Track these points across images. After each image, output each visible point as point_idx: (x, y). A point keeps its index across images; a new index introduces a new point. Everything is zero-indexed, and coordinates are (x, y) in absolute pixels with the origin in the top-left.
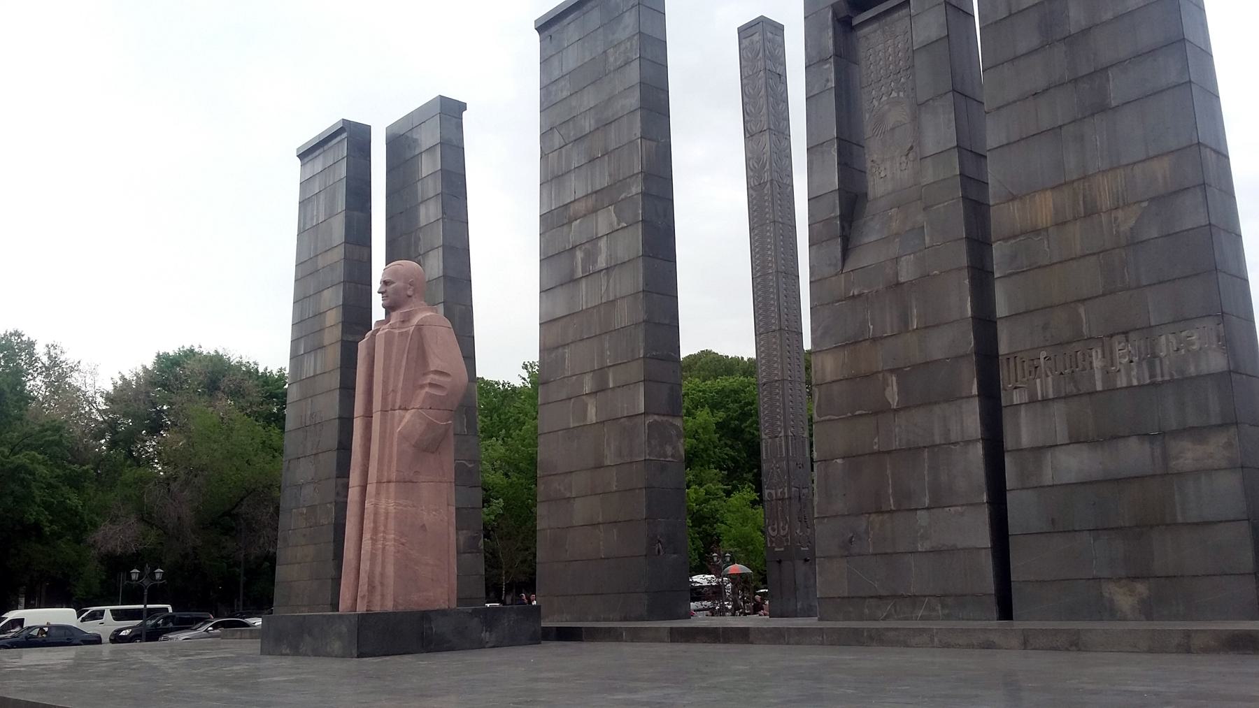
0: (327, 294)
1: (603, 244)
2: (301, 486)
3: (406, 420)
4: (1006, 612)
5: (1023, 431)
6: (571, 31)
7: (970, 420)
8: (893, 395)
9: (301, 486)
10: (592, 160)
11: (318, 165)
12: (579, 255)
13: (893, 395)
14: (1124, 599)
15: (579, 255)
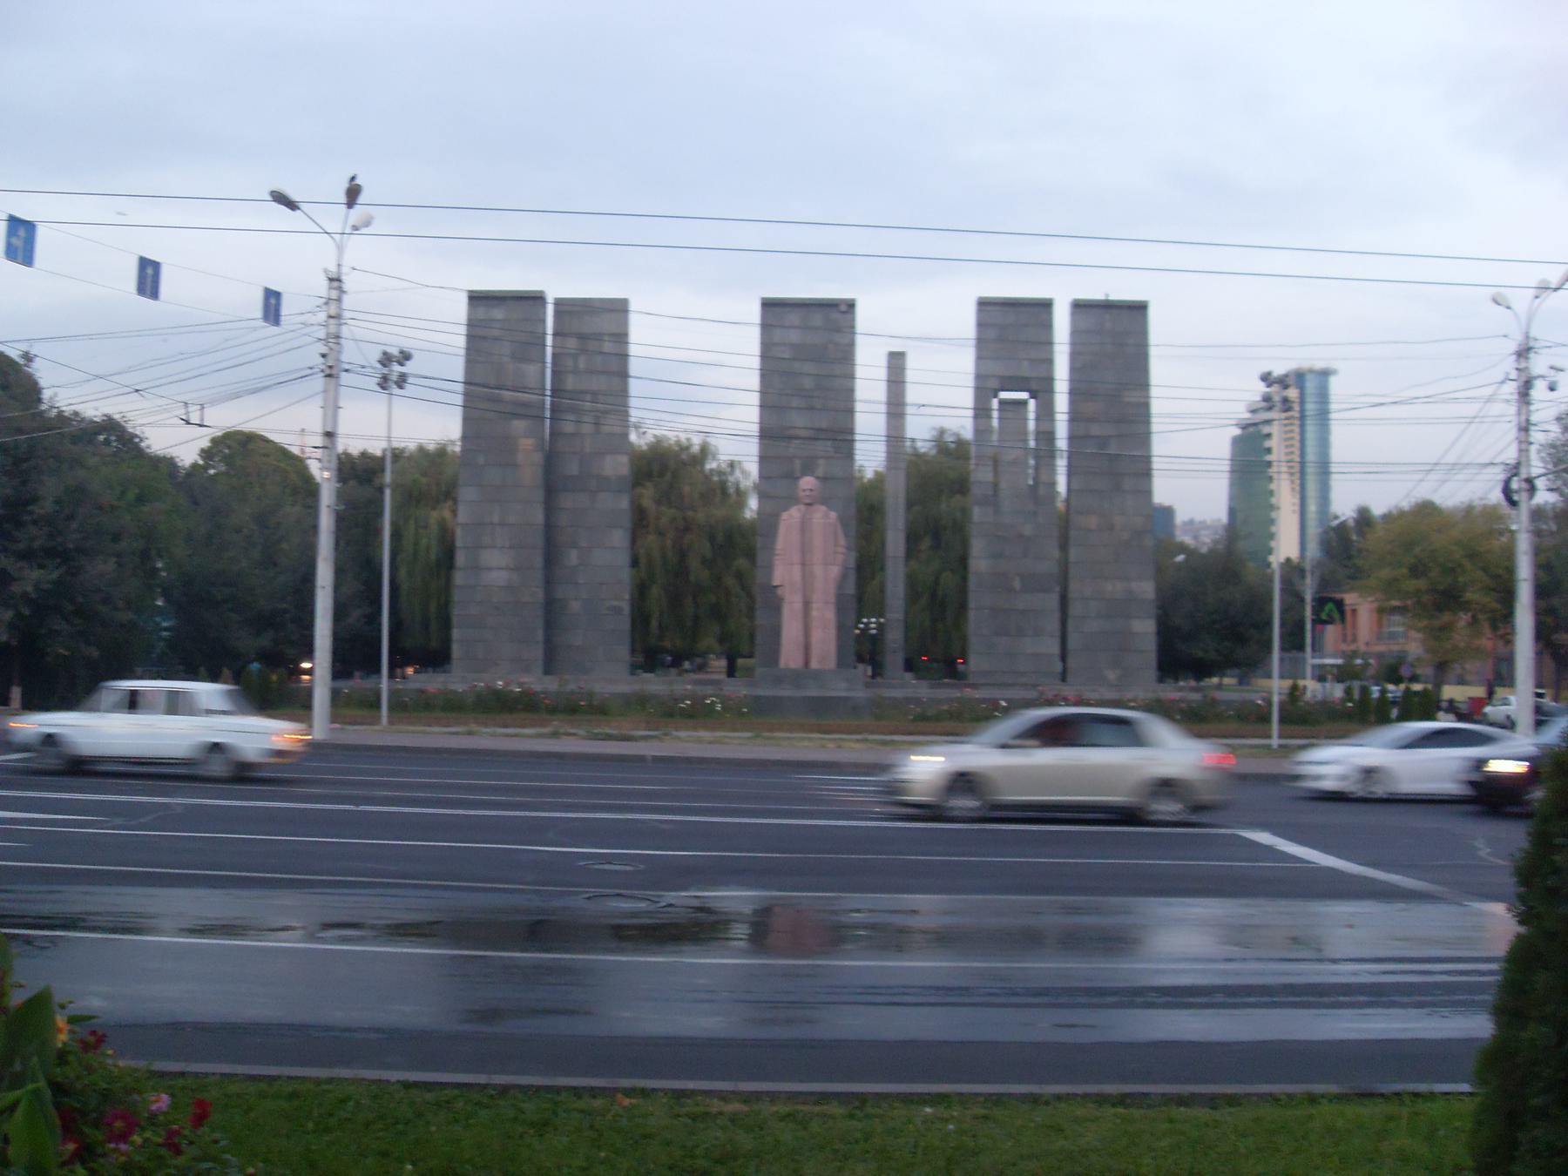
0: (519, 425)
1: (821, 462)
2: (490, 569)
3: (835, 571)
4: (1064, 679)
5: (1075, 609)
6: (794, 318)
7: (1052, 601)
8: (1017, 584)
9: (490, 569)
10: (812, 408)
11: (498, 313)
12: (798, 462)
13: (1017, 584)
14: (1111, 675)
15: (798, 462)
